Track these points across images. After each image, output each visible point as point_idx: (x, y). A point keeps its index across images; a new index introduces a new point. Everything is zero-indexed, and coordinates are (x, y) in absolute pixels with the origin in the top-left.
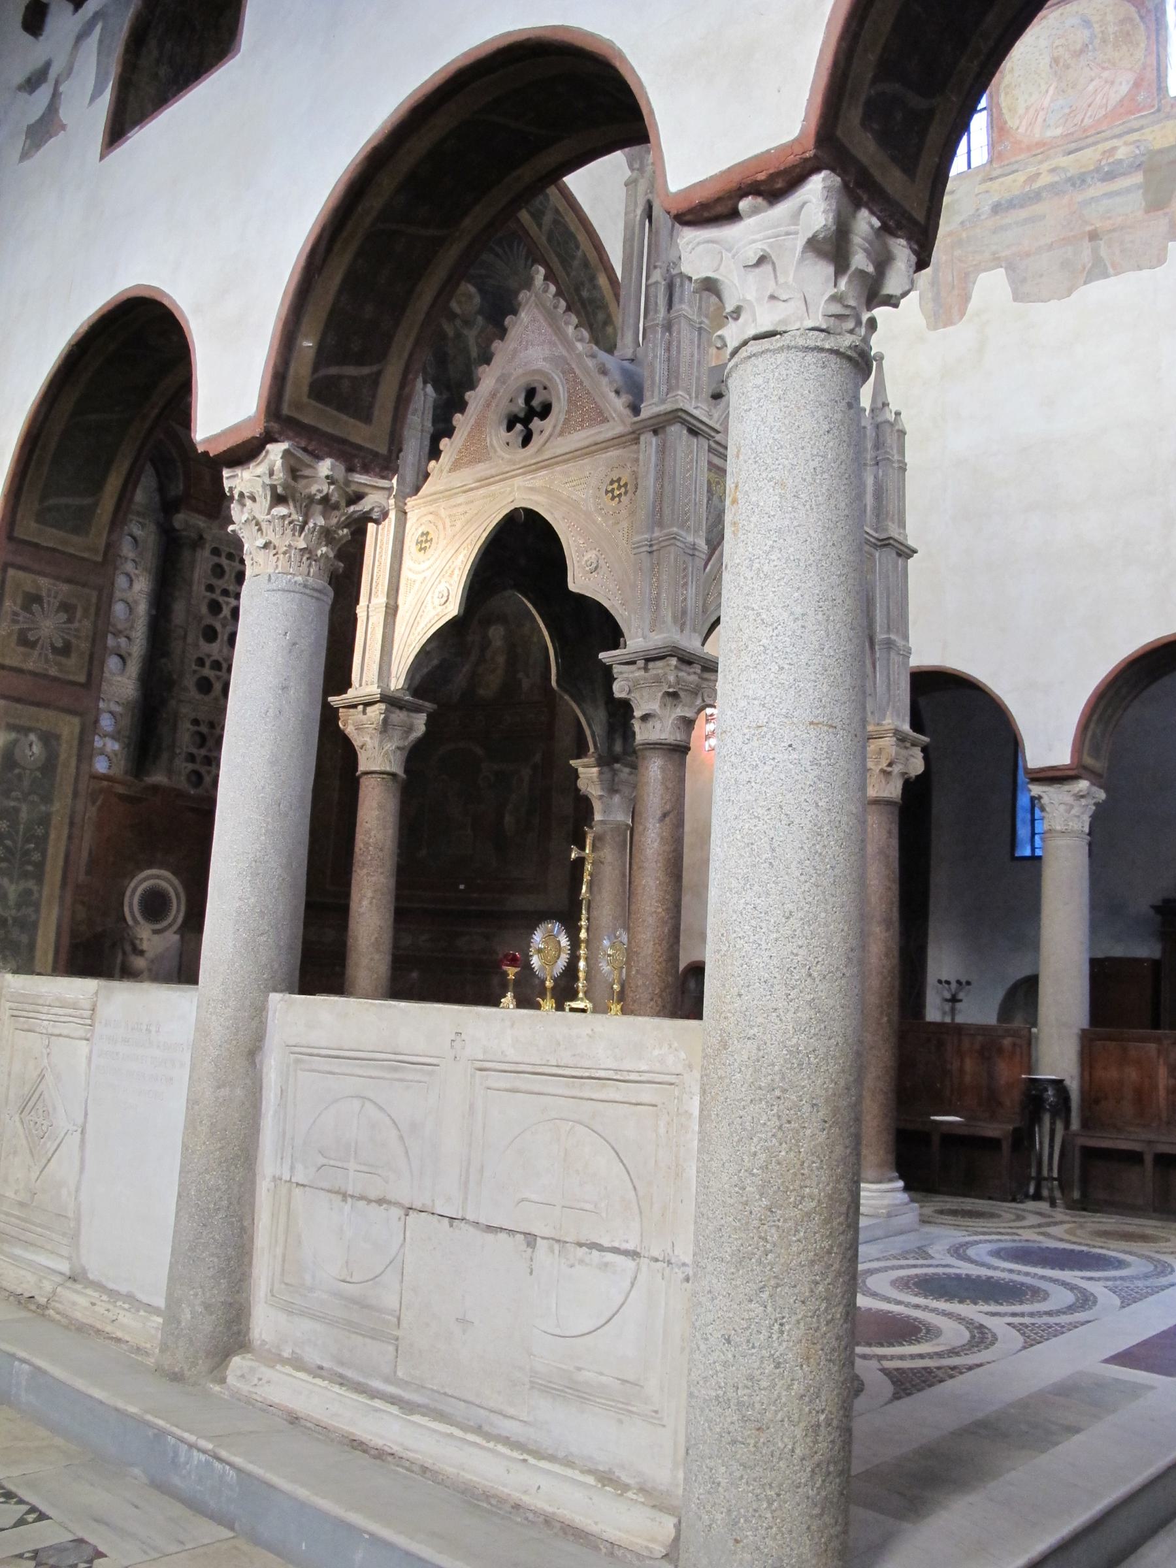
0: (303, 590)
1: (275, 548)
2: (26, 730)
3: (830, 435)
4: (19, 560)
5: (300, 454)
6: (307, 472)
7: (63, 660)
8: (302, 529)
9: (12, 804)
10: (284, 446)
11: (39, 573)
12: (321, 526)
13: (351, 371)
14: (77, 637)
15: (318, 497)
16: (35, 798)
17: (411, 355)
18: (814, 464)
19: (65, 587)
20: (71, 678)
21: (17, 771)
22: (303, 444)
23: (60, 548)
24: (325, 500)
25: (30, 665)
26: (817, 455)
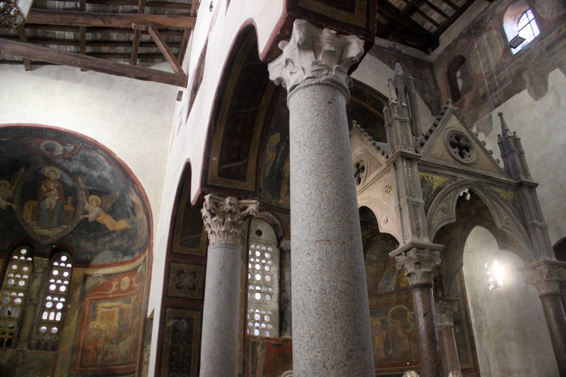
0: (225, 246)
1: (214, 232)
2: (179, 318)
3: (319, 116)
5: (217, 197)
6: (222, 203)
7: (193, 292)
8: (223, 224)
9: (177, 345)
10: (209, 195)
11: (182, 263)
12: (230, 222)
13: (235, 164)
14: (198, 283)
15: (227, 211)
16: (186, 343)
17: (258, 154)
18: (312, 129)
19: (192, 266)
20: (197, 298)
21: (178, 333)
22: (218, 194)
24: (230, 211)
25: (181, 295)
26: (313, 125)
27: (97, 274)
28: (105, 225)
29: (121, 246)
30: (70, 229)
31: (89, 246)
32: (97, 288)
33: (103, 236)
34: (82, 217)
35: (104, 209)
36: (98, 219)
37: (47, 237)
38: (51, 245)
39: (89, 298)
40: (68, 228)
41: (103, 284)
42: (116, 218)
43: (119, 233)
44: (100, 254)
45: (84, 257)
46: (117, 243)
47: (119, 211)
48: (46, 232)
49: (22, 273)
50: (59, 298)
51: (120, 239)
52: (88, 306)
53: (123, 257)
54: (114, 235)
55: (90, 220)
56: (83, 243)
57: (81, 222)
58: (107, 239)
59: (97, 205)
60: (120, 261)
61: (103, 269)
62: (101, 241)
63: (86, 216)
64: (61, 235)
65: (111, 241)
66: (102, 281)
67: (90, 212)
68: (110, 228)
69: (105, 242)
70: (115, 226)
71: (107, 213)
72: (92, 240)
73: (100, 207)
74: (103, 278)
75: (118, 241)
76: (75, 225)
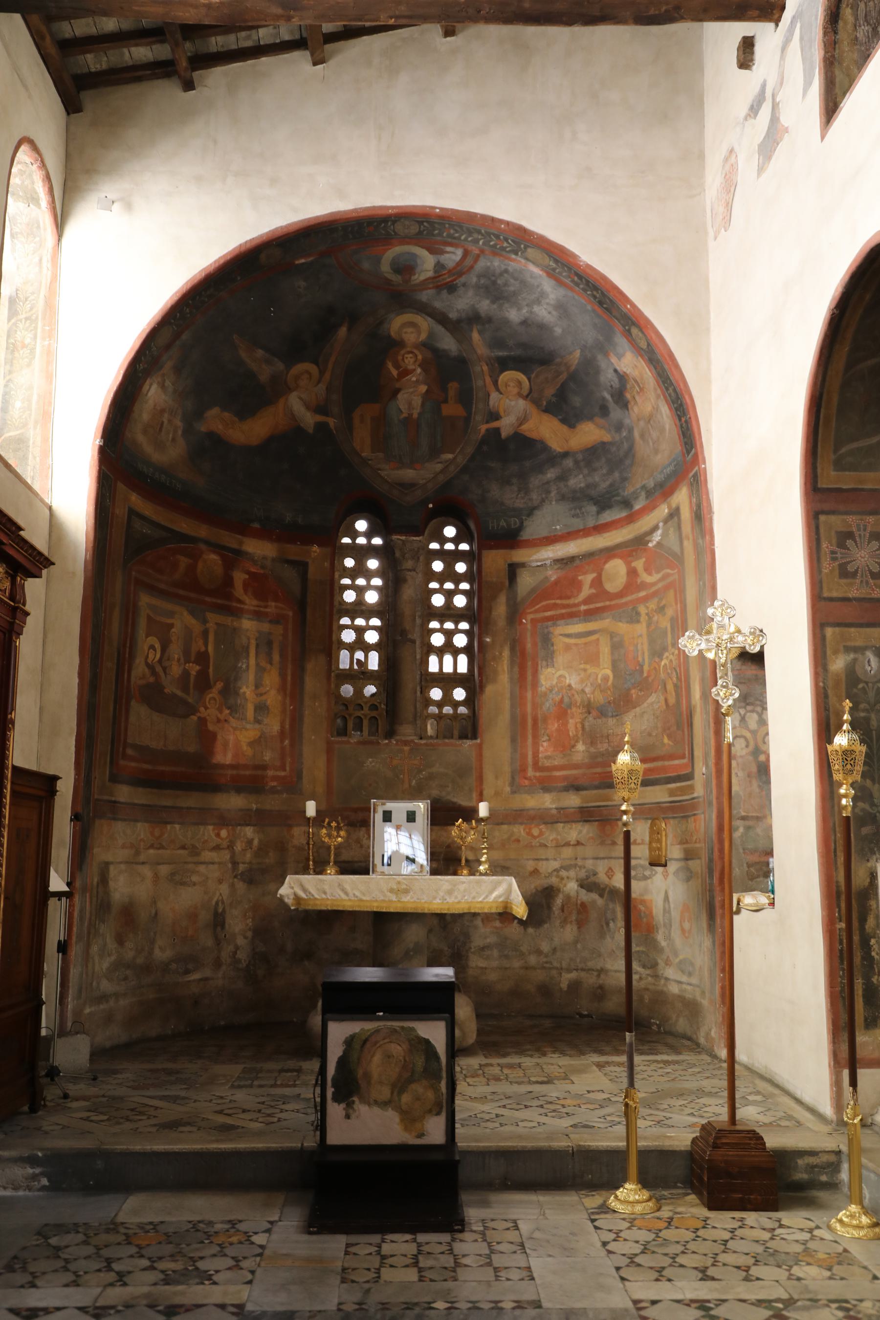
4: (826, 507)
23: (860, 487)
27: (537, 561)
28: (542, 442)
29: (588, 486)
30: (461, 460)
31: (511, 497)
32: (543, 593)
33: (540, 469)
34: (483, 428)
35: (536, 403)
36: (524, 427)
37: (412, 485)
38: (425, 502)
39: (530, 617)
40: (455, 458)
41: (556, 583)
42: (570, 420)
43: (580, 457)
44: (537, 512)
45: (503, 523)
46: (577, 481)
47: (576, 401)
48: (408, 474)
49: (368, 575)
50: (456, 624)
51: (586, 471)
52: (529, 634)
53: (598, 513)
54: (569, 463)
55: (504, 434)
56: (495, 491)
57: (484, 441)
58: (551, 474)
59: (520, 395)
60: (591, 523)
61: (550, 548)
62: (535, 481)
63: (495, 424)
64: (442, 478)
65: (563, 478)
66: (553, 575)
67: (502, 414)
68: (556, 445)
69: (548, 483)
70: (567, 441)
71: (546, 411)
72: (514, 480)
73: (526, 398)
74: (556, 567)
75: (581, 476)
76: (470, 450)
